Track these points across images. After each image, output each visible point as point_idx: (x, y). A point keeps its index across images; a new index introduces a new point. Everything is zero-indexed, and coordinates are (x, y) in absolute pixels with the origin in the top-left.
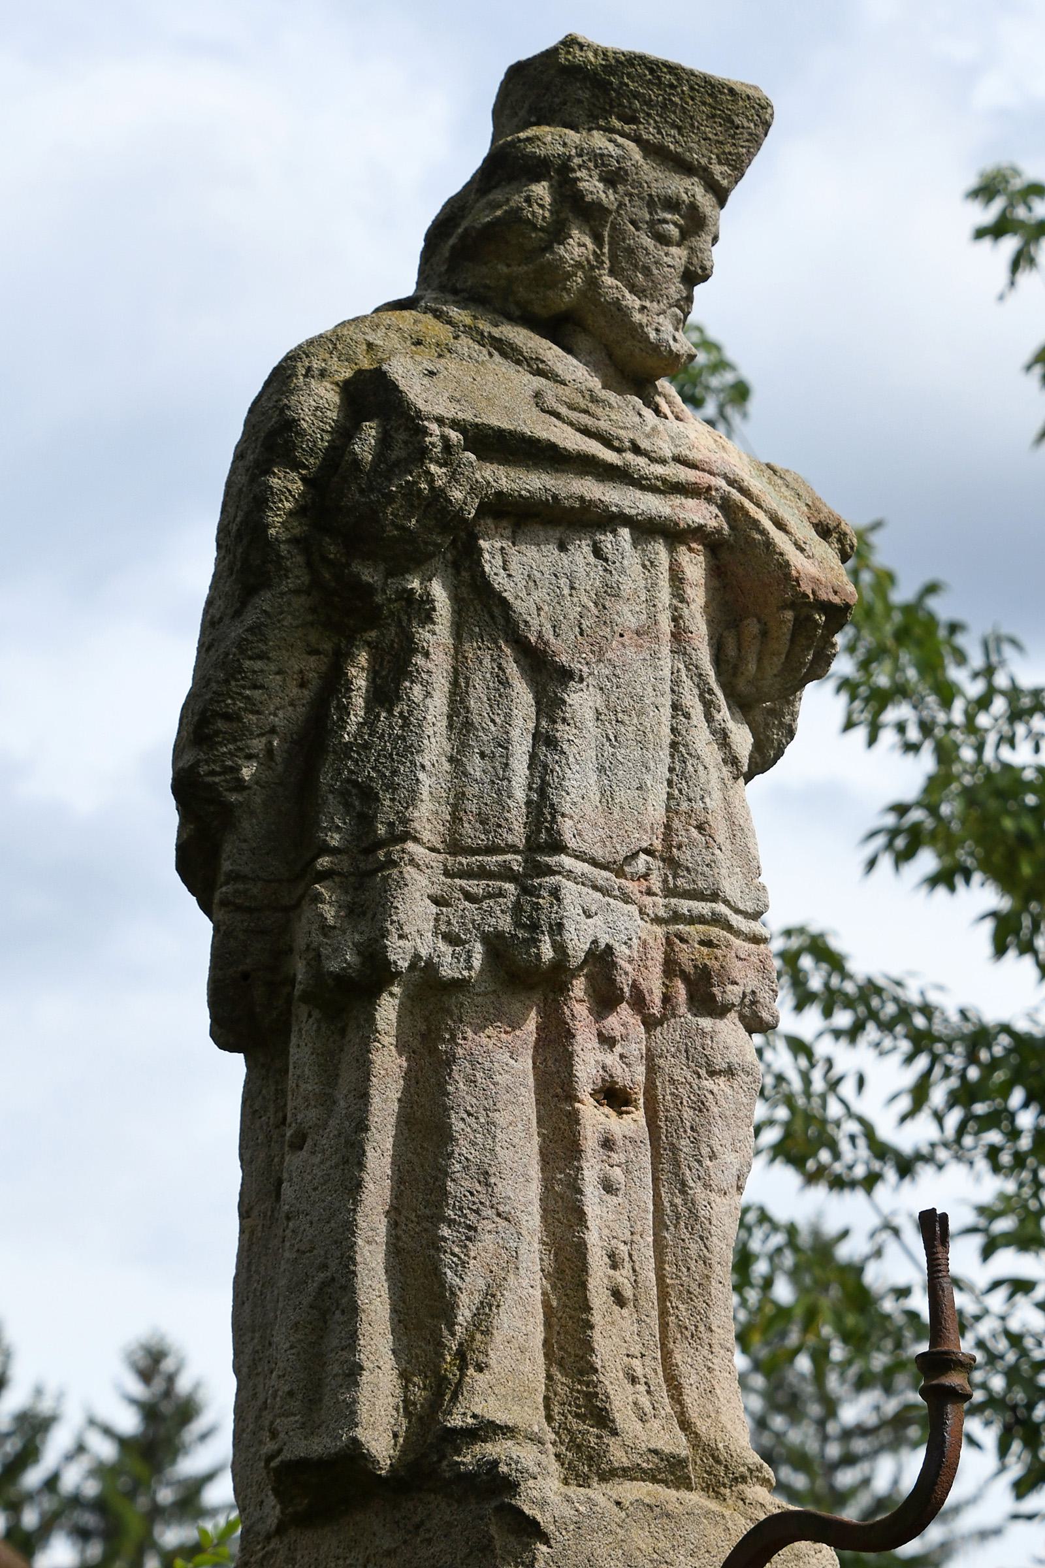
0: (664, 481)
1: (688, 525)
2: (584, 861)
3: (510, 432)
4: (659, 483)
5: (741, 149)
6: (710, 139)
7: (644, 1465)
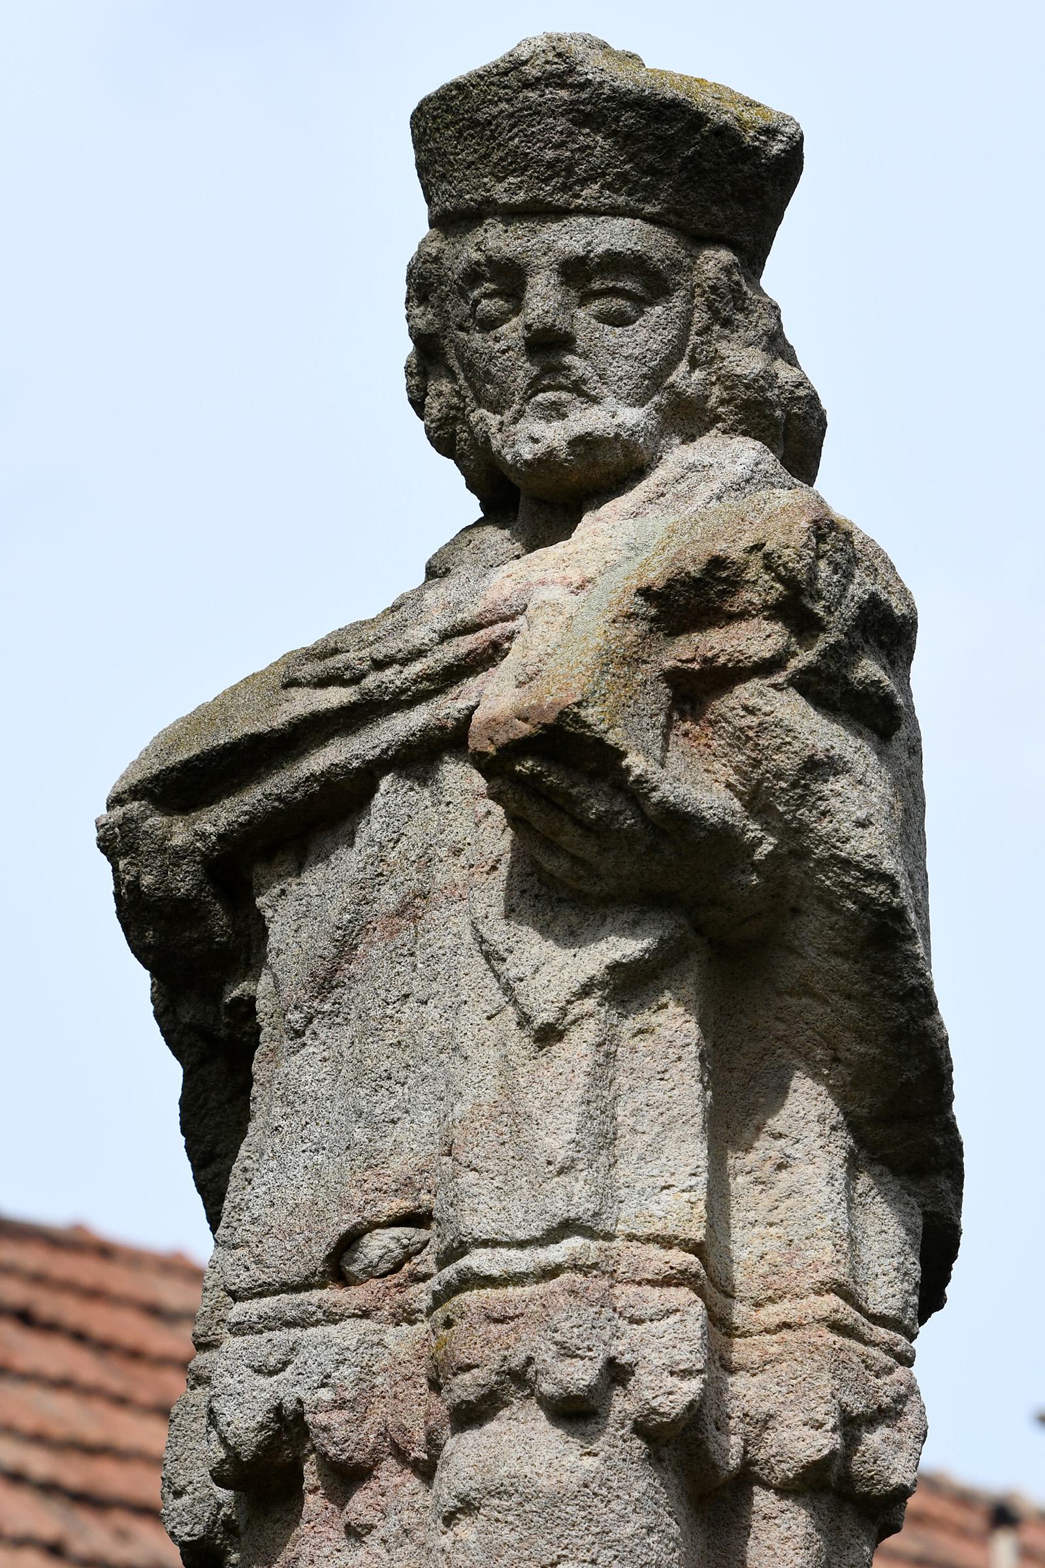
0: (427, 677)
1: (456, 719)
2: (276, 1293)
4: (425, 685)
6: (473, 163)
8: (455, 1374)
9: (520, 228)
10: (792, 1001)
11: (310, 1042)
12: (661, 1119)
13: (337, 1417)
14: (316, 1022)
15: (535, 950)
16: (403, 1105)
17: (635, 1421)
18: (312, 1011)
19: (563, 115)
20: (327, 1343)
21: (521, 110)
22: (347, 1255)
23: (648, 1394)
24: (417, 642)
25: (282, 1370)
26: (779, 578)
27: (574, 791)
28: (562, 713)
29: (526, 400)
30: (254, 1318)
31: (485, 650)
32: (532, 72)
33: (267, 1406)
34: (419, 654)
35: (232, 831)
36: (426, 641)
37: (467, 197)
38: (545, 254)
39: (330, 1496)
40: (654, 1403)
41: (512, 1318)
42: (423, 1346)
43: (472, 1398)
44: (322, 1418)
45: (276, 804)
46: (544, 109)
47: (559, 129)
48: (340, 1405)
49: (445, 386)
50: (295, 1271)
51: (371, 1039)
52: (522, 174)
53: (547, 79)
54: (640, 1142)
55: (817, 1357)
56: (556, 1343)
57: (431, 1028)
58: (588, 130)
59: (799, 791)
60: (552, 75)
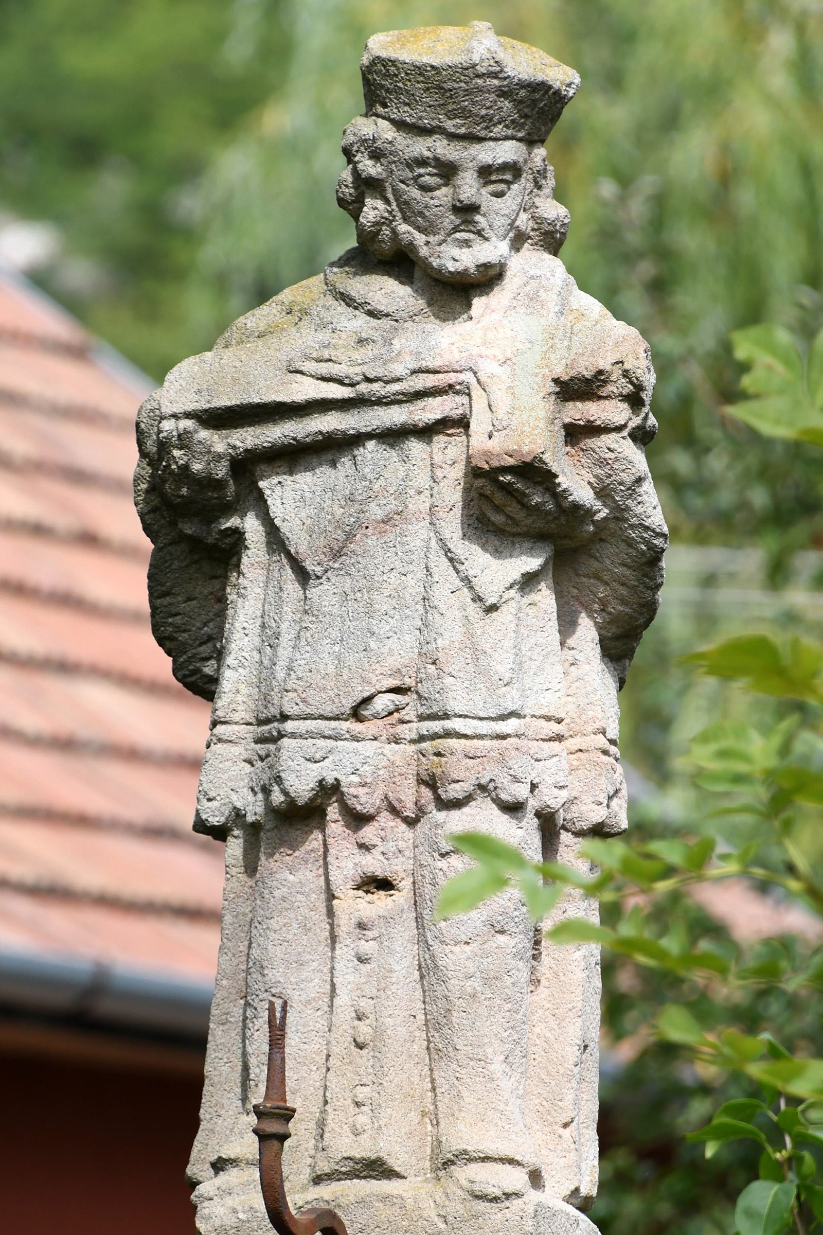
2: (315, 719)
3: (238, 406)
5: (463, 103)
7: (343, 1169)
8: (449, 784)
9: (459, 145)
10: (585, 580)
11: (325, 583)
12: (543, 653)
13: (361, 791)
14: (329, 572)
15: (481, 560)
16: (394, 629)
17: (537, 810)
18: (328, 567)
19: (493, 92)
20: (356, 753)
21: (473, 89)
22: (363, 706)
23: (546, 798)
24: (398, 375)
25: (323, 761)
26: (631, 383)
27: (527, 491)
28: (535, 457)
29: (449, 235)
30: (304, 732)
31: (444, 387)
32: (481, 69)
33: (316, 779)
34: (399, 380)
35: (257, 449)
36: (404, 374)
37: (426, 121)
38: (471, 161)
39: (348, 826)
40: (549, 803)
41: (479, 757)
42: (411, 759)
43: (461, 797)
44: (353, 791)
45: (291, 441)
46: (485, 89)
47: (491, 99)
48: (364, 785)
49: (380, 204)
50: (328, 710)
51: (376, 593)
53: (489, 74)
54: (534, 665)
55: (598, 769)
56: (511, 775)
57: (411, 590)
58: (502, 99)
59: (630, 492)
60: (492, 73)
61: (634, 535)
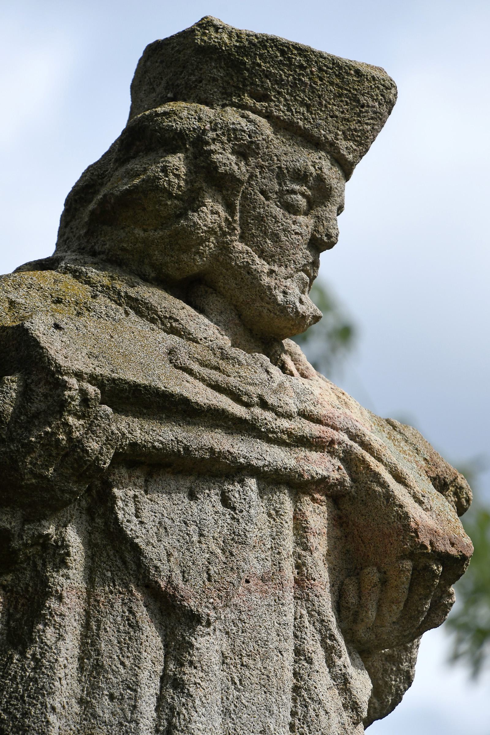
0: (290, 434)
1: (313, 477)
4: (285, 437)
5: (365, 126)
6: (337, 117)
52: (357, 146)
61: (393, 682)
